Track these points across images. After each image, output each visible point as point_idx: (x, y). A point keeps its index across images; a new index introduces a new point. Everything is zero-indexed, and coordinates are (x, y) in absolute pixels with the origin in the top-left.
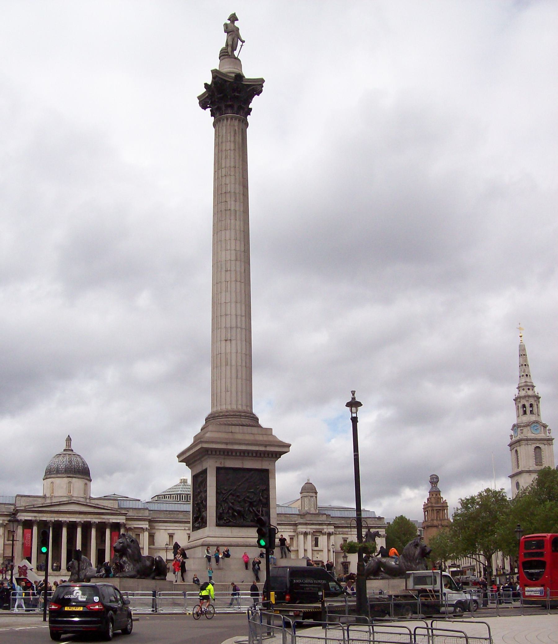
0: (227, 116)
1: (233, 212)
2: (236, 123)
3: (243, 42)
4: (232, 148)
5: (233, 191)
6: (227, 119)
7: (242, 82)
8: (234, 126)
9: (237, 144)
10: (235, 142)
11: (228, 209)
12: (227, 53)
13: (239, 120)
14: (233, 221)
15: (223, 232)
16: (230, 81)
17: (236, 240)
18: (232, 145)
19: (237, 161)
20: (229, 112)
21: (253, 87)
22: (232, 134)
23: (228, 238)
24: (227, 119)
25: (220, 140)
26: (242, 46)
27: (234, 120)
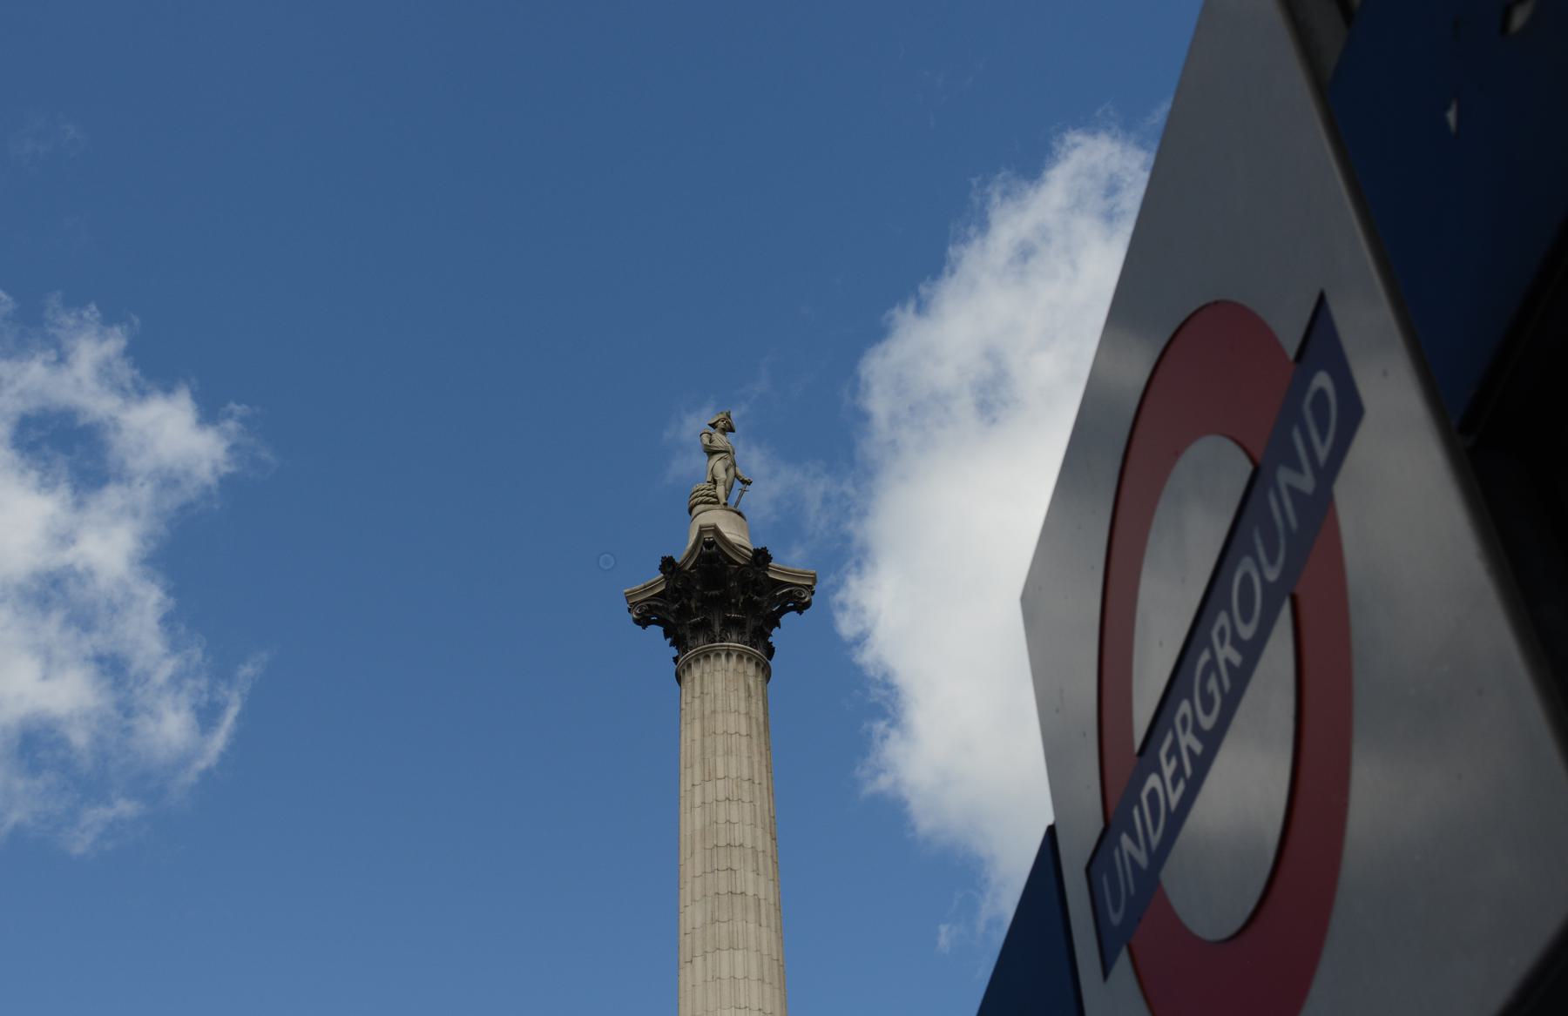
0: (729, 646)
1: (751, 902)
2: (751, 669)
3: (749, 483)
4: (744, 732)
5: (748, 843)
6: (728, 655)
7: (766, 572)
8: (745, 672)
9: (754, 721)
10: (748, 714)
11: (739, 892)
12: (714, 500)
13: (757, 665)
14: (752, 926)
15: (725, 954)
16: (737, 563)
17: (761, 980)
18: (743, 721)
19: (756, 766)
20: (734, 637)
21: (793, 588)
22: (743, 694)
23: (739, 974)
24: (728, 655)
25: (708, 705)
26: (743, 491)
27: (745, 660)
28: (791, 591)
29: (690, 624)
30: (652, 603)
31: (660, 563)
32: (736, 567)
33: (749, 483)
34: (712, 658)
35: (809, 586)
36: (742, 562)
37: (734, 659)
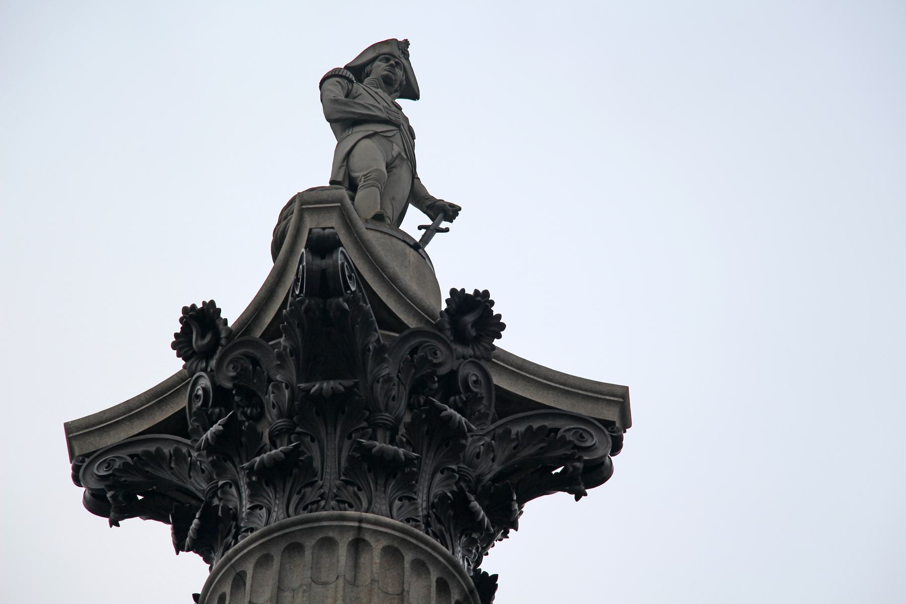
0: (360, 520)
3: (449, 212)
16: (398, 325)
26: (430, 232)
29: (251, 471)
30: (139, 450)
31: (178, 328)
32: (397, 335)
33: (449, 212)
34: (308, 553)
35: (609, 424)
36: (411, 323)
37: (374, 558)
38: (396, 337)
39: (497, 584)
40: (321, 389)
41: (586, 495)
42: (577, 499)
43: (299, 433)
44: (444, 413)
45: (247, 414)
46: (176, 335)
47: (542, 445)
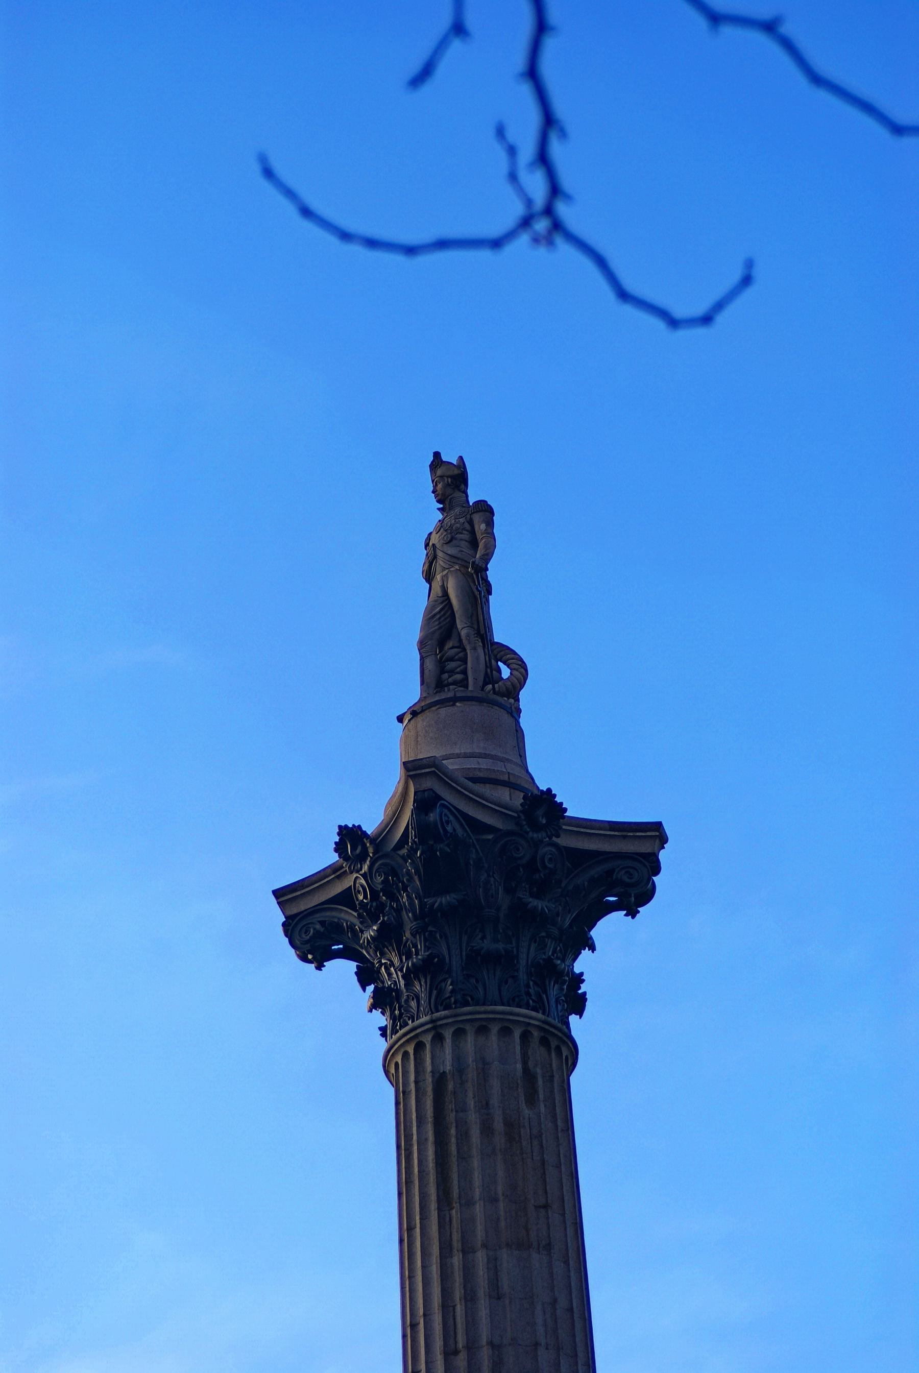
28: (610, 873)
38: (489, 840)
39: (587, 999)
40: (441, 903)
41: (638, 912)
42: (633, 917)
43: (431, 931)
44: (530, 906)
45: (394, 907)
46: (336, 843)
47: (603, 888)
